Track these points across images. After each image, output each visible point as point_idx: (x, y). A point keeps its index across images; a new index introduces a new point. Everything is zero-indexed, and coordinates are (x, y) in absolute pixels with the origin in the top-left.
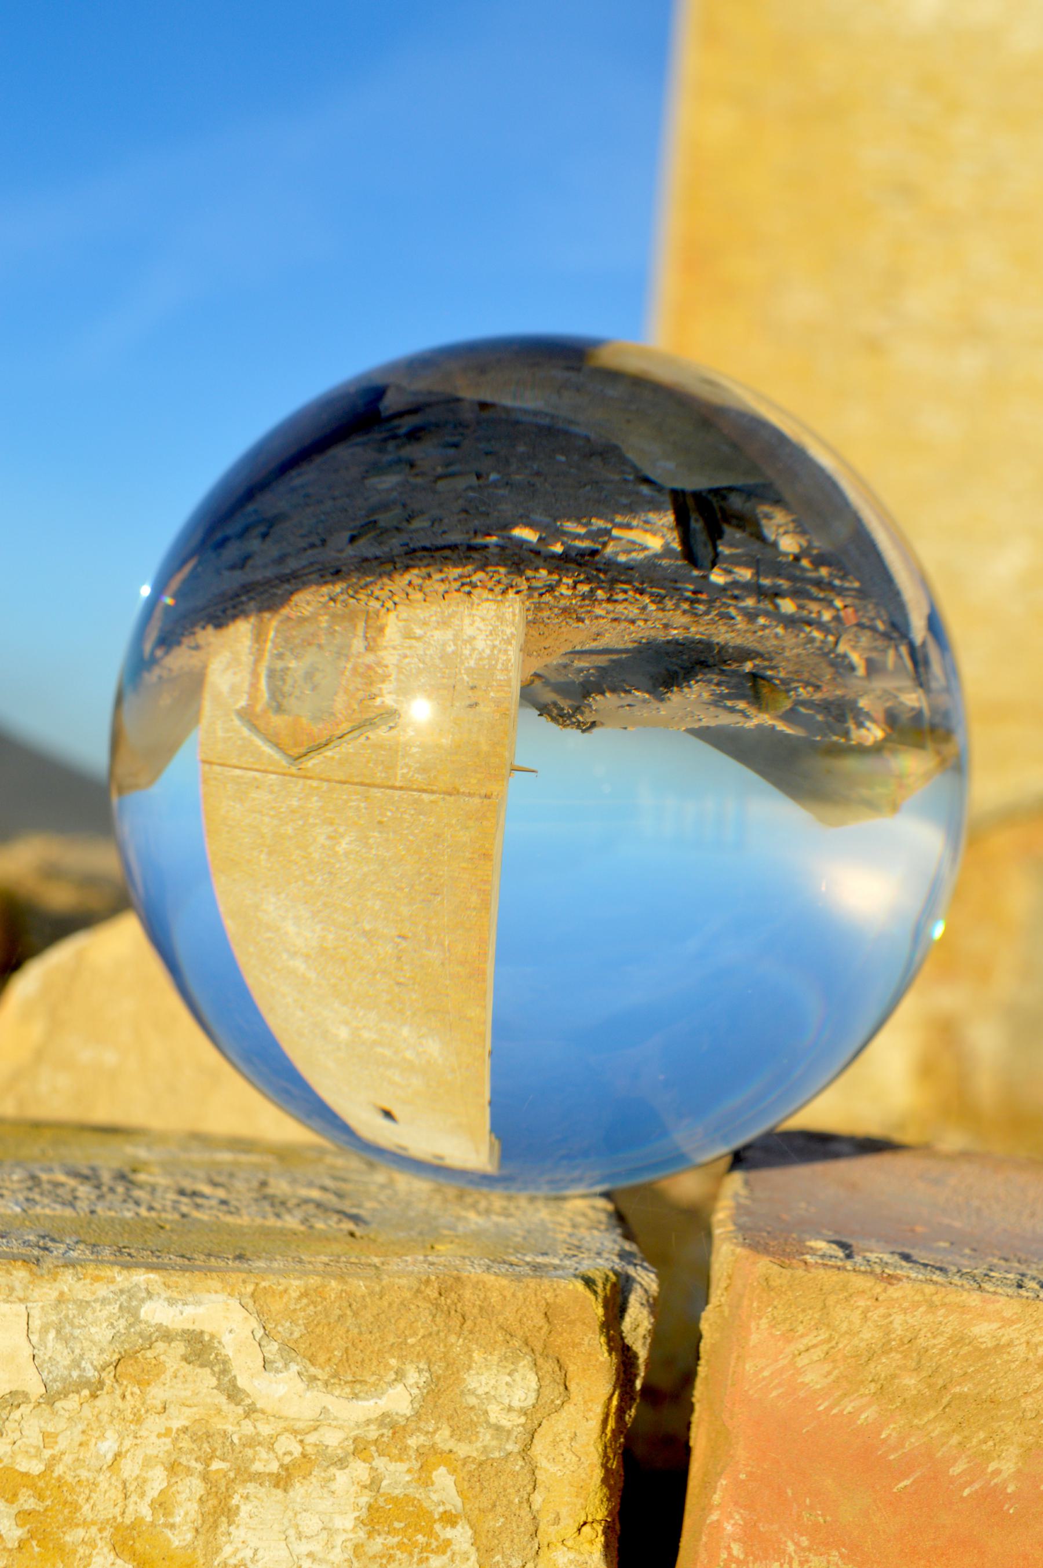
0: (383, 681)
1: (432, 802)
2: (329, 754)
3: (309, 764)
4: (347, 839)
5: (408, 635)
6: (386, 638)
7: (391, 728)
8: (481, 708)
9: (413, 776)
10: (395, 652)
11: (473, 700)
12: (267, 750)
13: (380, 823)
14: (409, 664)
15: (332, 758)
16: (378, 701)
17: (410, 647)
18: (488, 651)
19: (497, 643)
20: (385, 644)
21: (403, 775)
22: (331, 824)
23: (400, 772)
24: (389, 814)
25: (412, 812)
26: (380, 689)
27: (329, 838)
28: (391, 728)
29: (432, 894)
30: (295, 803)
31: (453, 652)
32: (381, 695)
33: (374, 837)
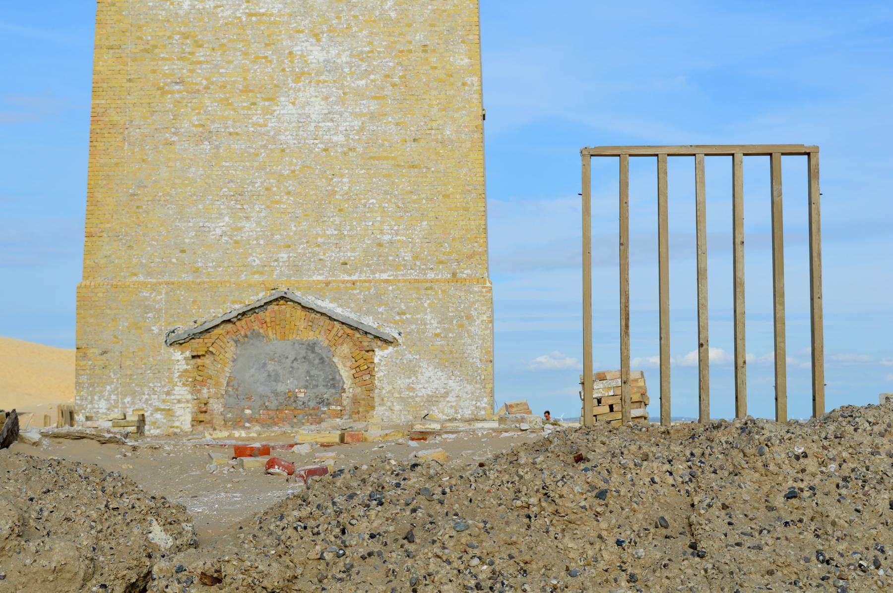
0: (186, 371)
1: (135, 275)
2: (237, 306)
3: (261, 295)
4: (218, 231)
5: (169, 412)
6: (188, 410)
7: (173, 332)
8: (97, 351)
9: (151, 294)
10: (178, 397)
11: (104, 357)
12: (326, 305)
13: (183, 251)
14: (164, 386)
15: (234, 302)
16: (188, 354)
17: (164, 401)
18: (96, 398)
19: (89, 406)
20: (190, 405)
21: (160, 293)
22: (236, 242)
23: (163, 296)
24: (174, 260)
25: (152, 265)
26: (187, 364)
27: (240, 229)
28: (173, 332)
29: (137, 195)
30: (284, 256)
31: (125, 396)
32: (185, 359)
33: (191, 238)
